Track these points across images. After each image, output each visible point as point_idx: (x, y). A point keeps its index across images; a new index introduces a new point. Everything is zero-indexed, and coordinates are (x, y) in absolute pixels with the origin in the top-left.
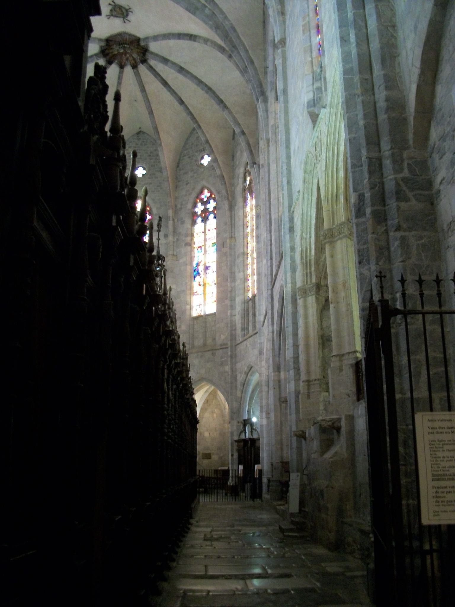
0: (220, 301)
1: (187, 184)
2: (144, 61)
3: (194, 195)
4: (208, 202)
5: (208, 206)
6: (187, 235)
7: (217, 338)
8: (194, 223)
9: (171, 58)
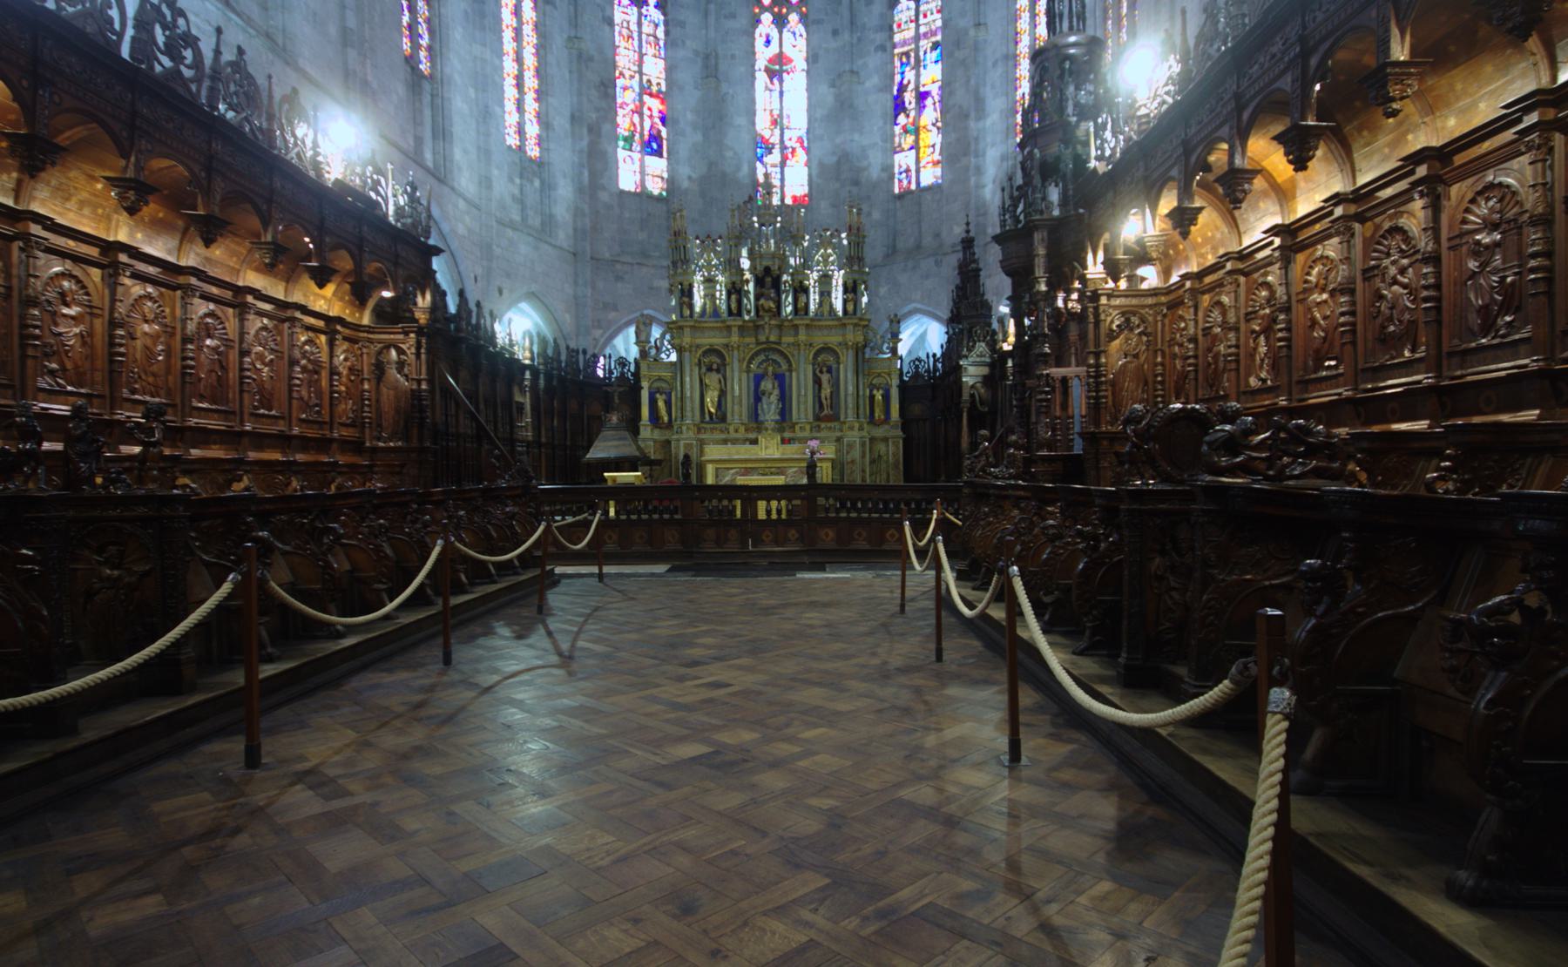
7: (944, 234)
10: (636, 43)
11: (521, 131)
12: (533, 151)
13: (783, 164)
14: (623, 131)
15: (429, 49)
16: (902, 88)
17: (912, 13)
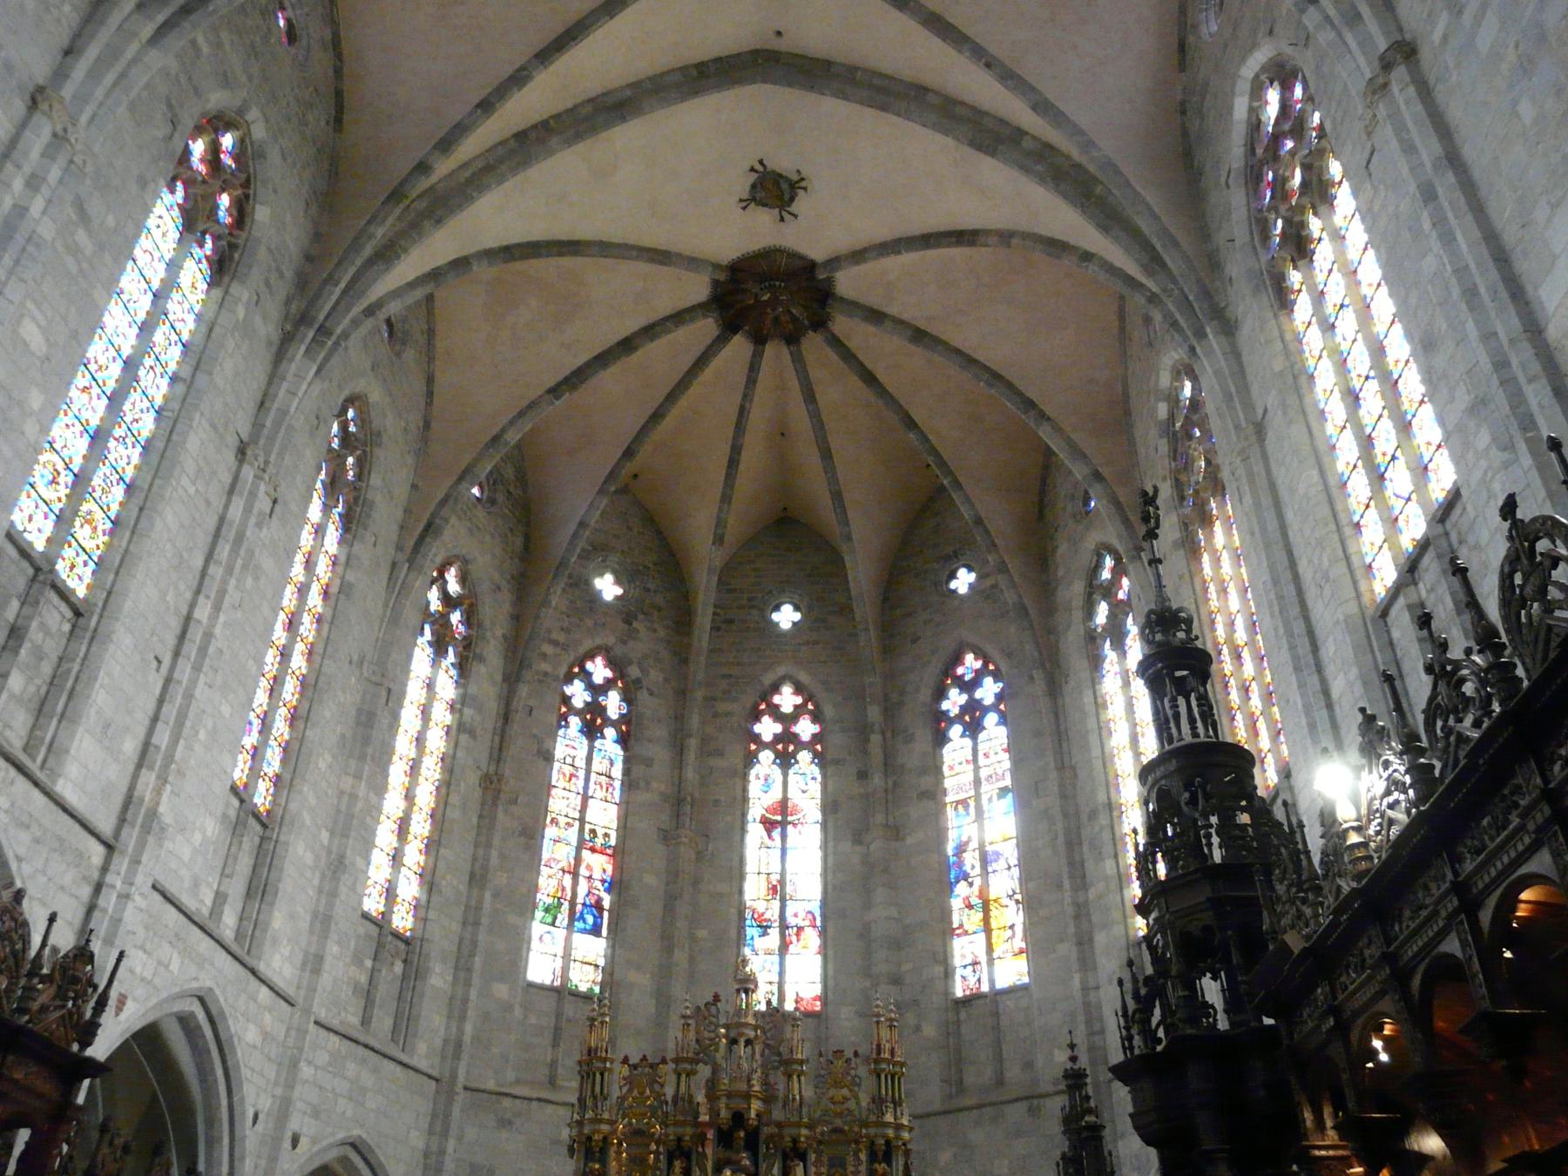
0: (1036, 948)
1: (914, 641)
2: (820, 324)
3: (936, 666)
4: (975, 683)
5: (978, 694)
6: (923, 771)
7: (1040, 1061)
8: (941, 739)
9: (893, 310)
10: (581, 783)
11: (390, 894)
12: (403, 920)
13: (784, 947)
14: (543, 898)
15: (277, 780)
16: (961, 849)
17: (969, 752)
